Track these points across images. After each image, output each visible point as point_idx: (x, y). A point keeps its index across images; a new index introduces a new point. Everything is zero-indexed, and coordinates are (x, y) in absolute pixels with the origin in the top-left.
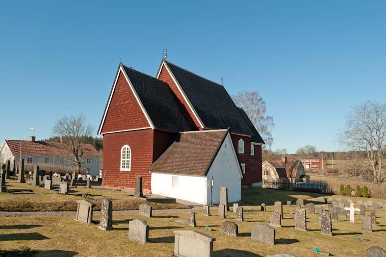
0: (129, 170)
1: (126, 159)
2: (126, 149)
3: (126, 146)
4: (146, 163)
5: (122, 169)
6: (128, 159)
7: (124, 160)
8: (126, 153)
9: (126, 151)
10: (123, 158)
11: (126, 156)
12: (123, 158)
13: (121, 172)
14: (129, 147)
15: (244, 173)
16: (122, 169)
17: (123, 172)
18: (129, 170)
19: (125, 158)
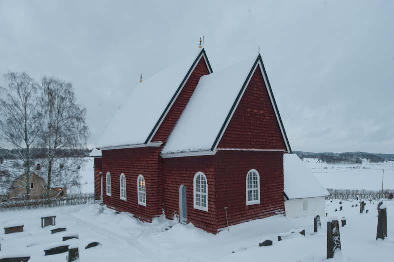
0: (258, 202)
1: (253, 189)
2: (252, 175)
3: (253, 171)
4: (273, 192)
5: (248, 203)
6: (250, 190)
7: (256, 189)
8: (253, 181)
9: (253, 177)
10: (257, 191)
11: (253, 185)
12: (248, 188)
13: (247, 208)
14: (257, 173)
15: (284, 197)
16: (248, 203)
17: (251, 207)
18: (258, 202)
19: (251, 188)
